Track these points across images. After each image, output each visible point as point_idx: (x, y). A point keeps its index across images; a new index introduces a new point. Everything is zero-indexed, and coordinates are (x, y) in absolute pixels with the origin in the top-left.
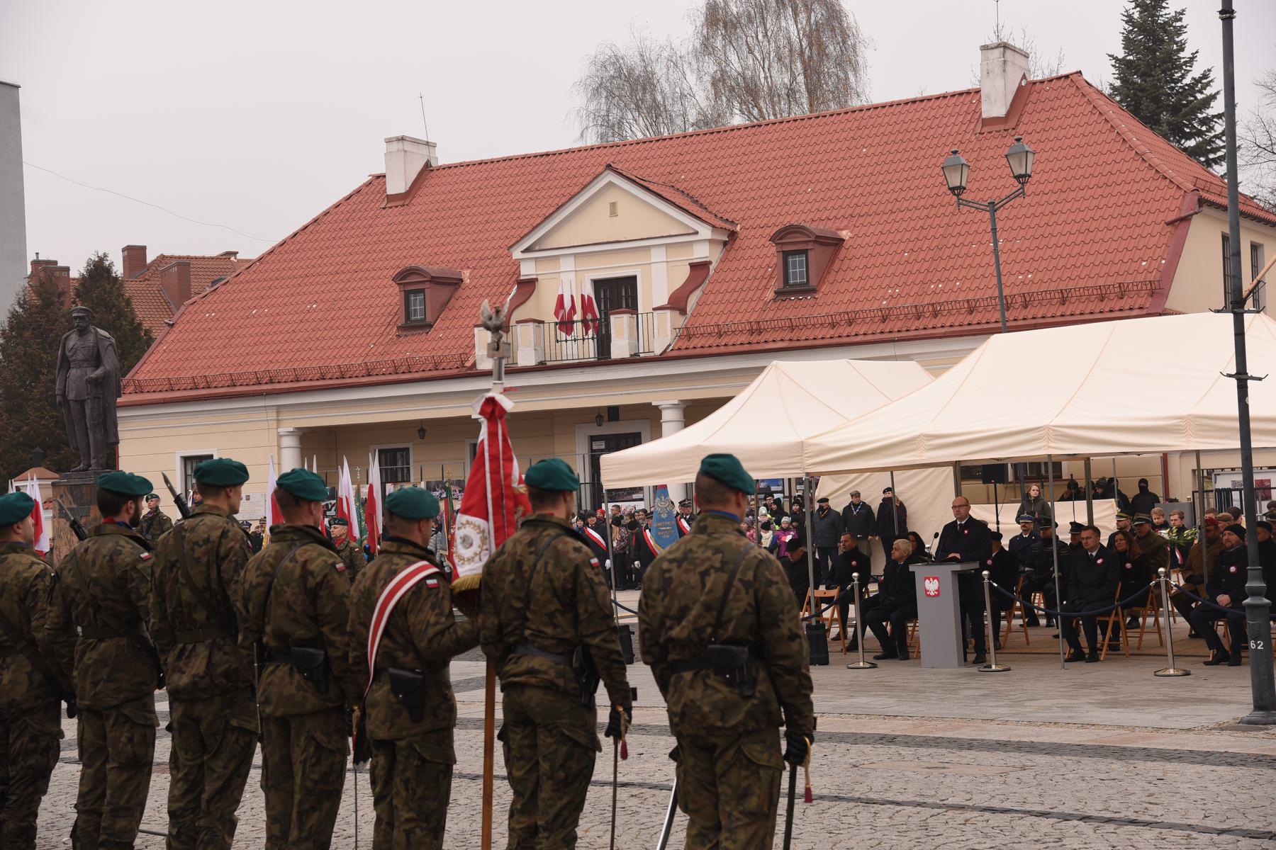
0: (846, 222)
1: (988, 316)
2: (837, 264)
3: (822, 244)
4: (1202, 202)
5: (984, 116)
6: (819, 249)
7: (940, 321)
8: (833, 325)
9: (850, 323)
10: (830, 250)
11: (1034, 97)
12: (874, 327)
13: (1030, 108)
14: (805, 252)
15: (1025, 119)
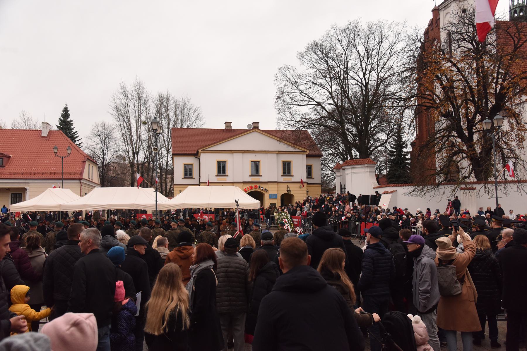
0: (11, 153)
1: (47, 176)
2: (9, 162)
3: (6, 157)
4: (88, 159)
5: (42, 135)
6: (6, 158)
7: (35, 176)
8: (10, 174)
9: (14, 174)
10: (8, 158)
11: (52, 134)
12: (20, 176)
13: (51, 136)
14: (3, 158)
15: (51, 137)
